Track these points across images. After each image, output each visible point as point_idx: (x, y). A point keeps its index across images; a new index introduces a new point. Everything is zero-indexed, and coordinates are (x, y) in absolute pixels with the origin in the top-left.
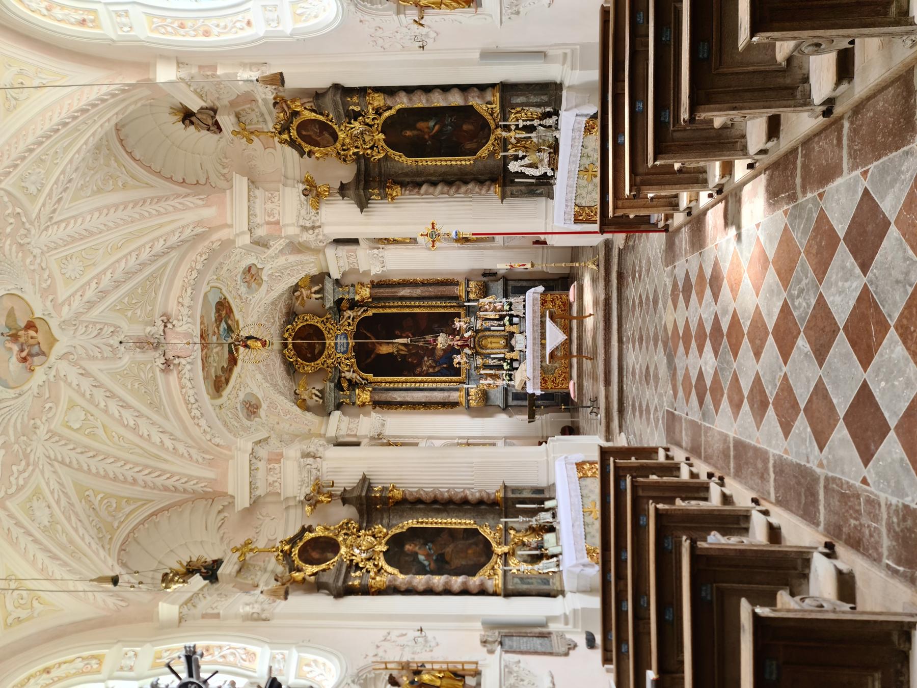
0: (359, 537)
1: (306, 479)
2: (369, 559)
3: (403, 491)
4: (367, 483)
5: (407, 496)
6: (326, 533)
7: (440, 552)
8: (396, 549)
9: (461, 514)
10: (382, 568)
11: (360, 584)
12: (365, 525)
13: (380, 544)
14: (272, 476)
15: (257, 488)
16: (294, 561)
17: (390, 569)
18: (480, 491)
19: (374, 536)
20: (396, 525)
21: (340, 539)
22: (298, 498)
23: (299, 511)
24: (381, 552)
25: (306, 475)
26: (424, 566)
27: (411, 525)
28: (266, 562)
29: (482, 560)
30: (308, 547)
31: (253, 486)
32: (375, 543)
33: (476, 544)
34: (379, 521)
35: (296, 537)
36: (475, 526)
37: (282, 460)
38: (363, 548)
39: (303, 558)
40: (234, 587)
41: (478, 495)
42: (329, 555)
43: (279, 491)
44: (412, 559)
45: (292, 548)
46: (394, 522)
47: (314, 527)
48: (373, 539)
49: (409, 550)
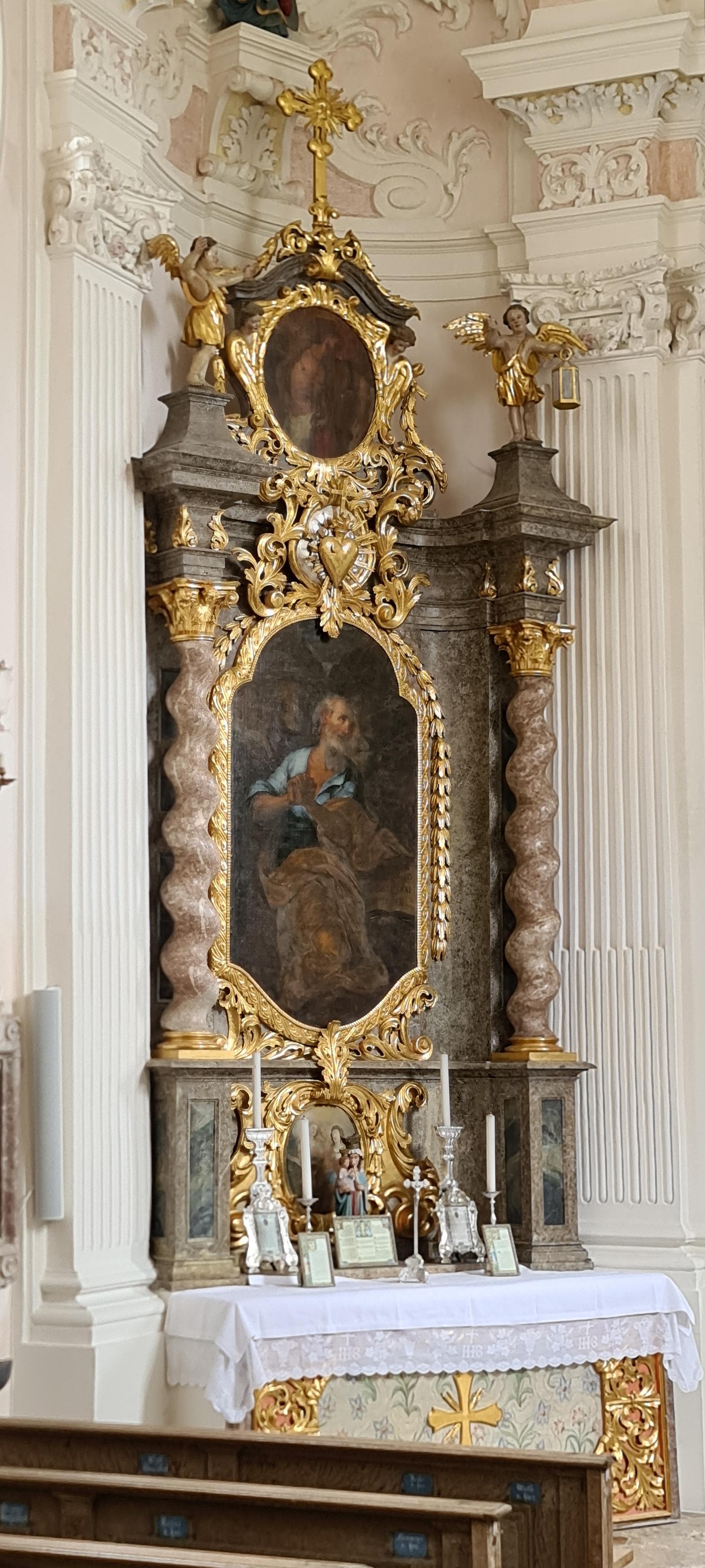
0: (372, 524)
1: (592, 301)
2: (287, 568)
3: (547, 679)
4: (574, 536)
5: (526, 695)
6: (386, 402)
7: (320, 830)
8: (328, 666)
9: (469, 900)
10: (259, 619)
11: (183, 548)
12: (420, 540)
13: (347, 606)
14: (603, 167)
15: (556, 117)
16: (281, 295)
17: (252, 650)
18: (551, 975)
19: (376, 578)
20: (423, 658)
21: (364, 454)
22: (517, 278)
23: (479, 288)
24: (319, 612)
25: (603, 299)
26: (268, 772)
27: (421, 712)
28: (285, 191)
29: (295, 987)
30: (332, 341)
31: (560, 102)
32: (349, 587)
33: (350, 965)
34: (437, 592)
35: (370, 287)
36: (422, 953)
37: (661, 198)
38: (328, 545)
39: (294, 328)
40: (195, 88)
41: (537, 965)
42: (304, 423)
43: (546, 203)
44: (292, 727)
45: (331, 282)
46: (434, 651)
47: (408, 352)
48: (362, 579)
49: (326, 712)
